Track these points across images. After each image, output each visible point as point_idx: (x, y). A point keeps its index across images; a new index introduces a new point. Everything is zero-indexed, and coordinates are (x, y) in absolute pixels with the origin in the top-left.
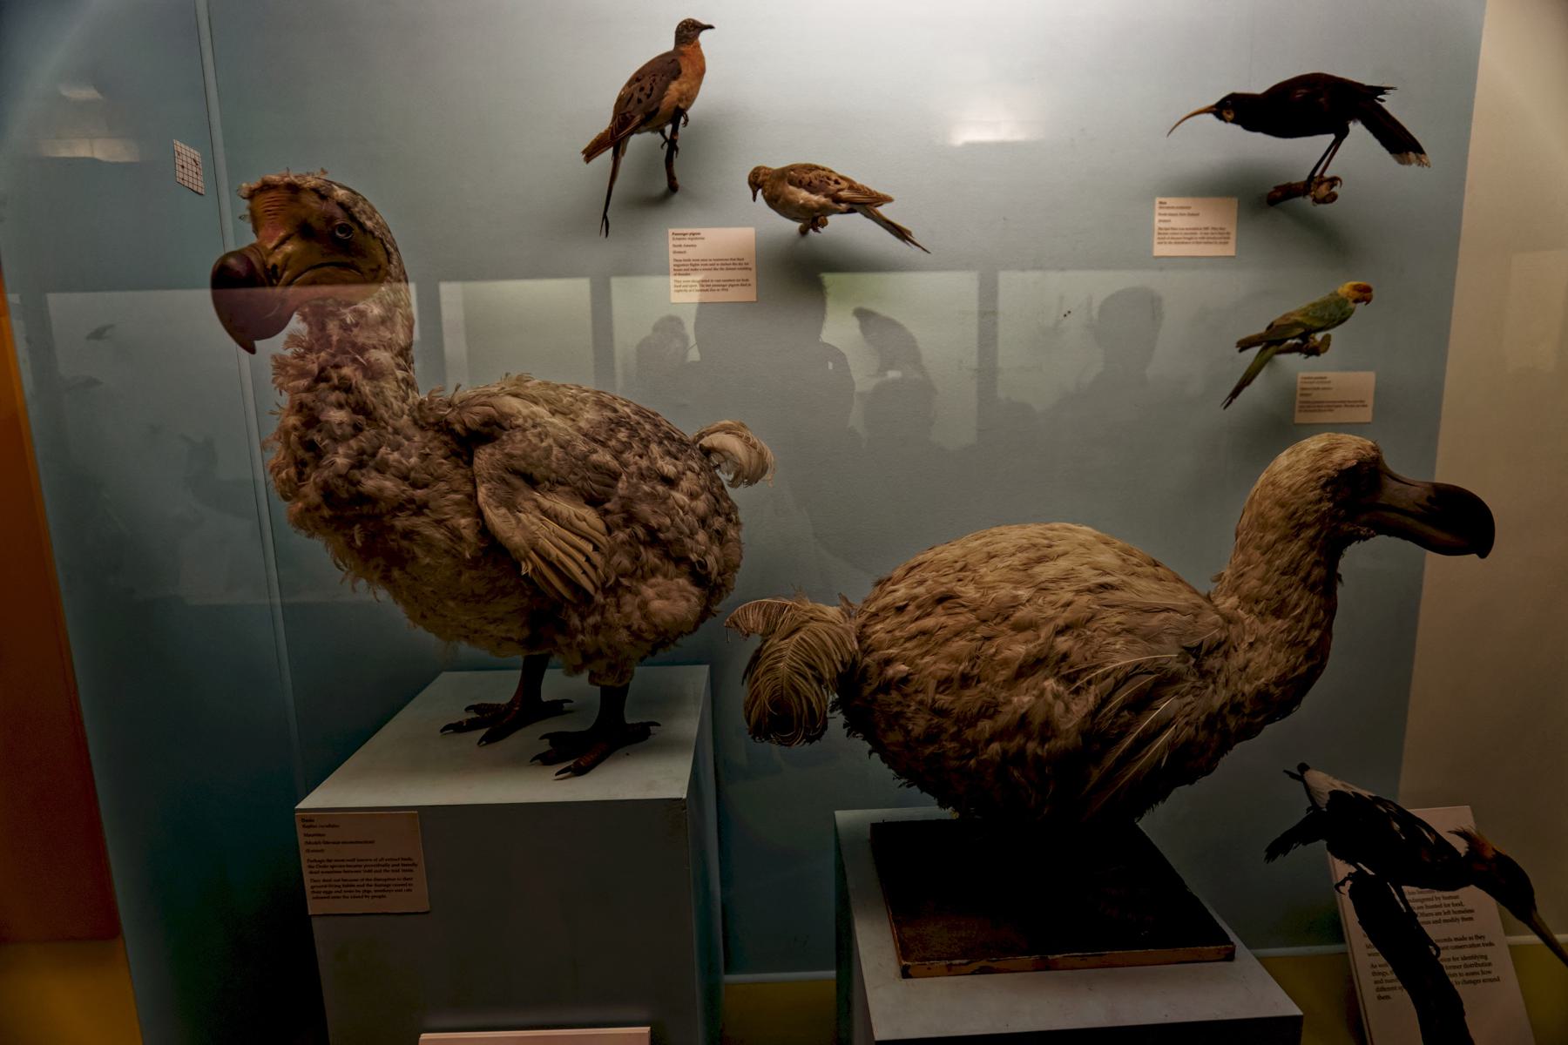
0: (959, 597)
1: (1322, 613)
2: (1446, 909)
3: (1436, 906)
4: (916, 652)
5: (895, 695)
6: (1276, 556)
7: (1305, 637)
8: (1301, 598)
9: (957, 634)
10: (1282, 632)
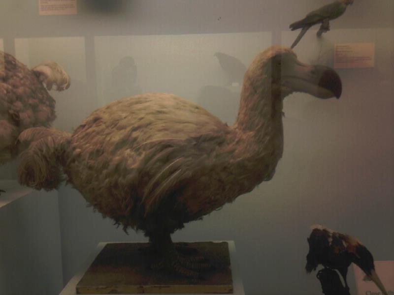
4: (84, 142)
5: (76, 163)
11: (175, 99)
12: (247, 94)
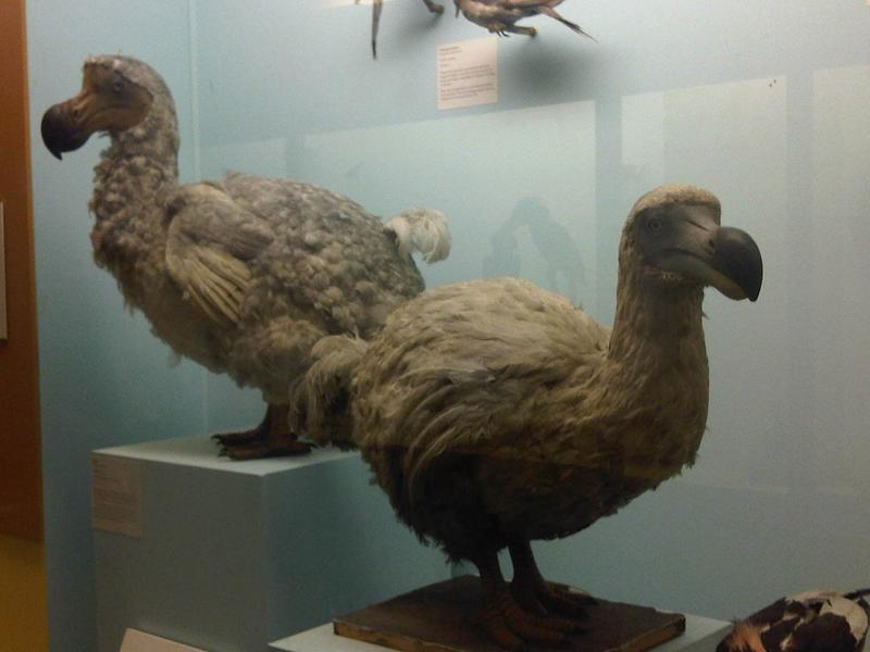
7: (635, 379)
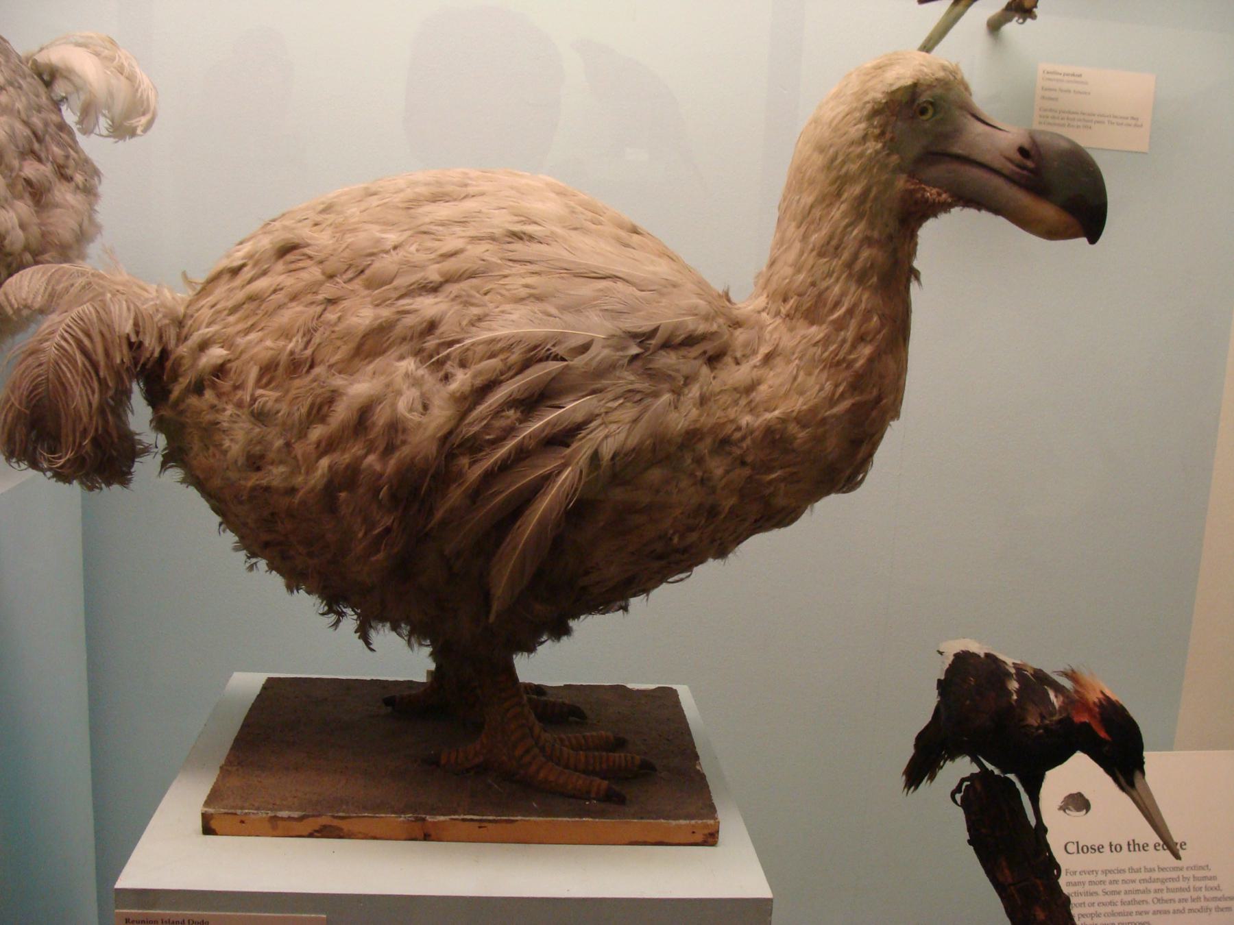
0: (308, 245)
1: (875, 319)
2: (1195, 895)
3: (1181, 890)
4: (241, 326)
5: (209, 395)
6: (812, 227)
7: (850, 352)
8: (843, 294)
9: (294, 298)
10: (816, 344)
11: (561, 193)
12: (808, 199)
